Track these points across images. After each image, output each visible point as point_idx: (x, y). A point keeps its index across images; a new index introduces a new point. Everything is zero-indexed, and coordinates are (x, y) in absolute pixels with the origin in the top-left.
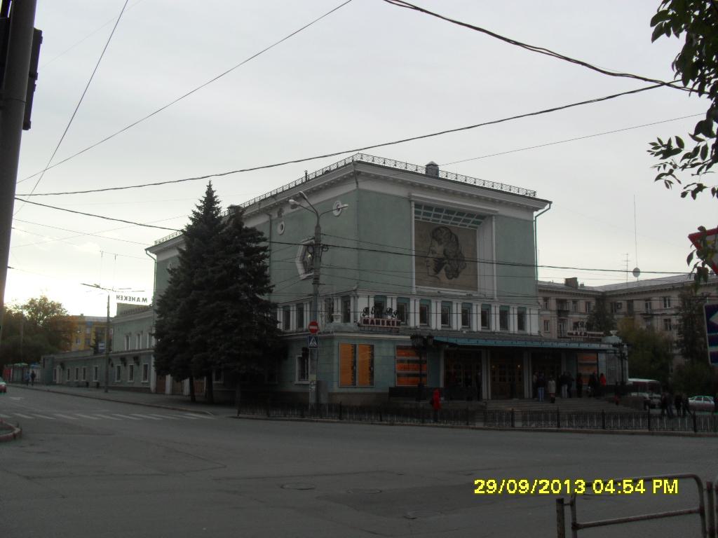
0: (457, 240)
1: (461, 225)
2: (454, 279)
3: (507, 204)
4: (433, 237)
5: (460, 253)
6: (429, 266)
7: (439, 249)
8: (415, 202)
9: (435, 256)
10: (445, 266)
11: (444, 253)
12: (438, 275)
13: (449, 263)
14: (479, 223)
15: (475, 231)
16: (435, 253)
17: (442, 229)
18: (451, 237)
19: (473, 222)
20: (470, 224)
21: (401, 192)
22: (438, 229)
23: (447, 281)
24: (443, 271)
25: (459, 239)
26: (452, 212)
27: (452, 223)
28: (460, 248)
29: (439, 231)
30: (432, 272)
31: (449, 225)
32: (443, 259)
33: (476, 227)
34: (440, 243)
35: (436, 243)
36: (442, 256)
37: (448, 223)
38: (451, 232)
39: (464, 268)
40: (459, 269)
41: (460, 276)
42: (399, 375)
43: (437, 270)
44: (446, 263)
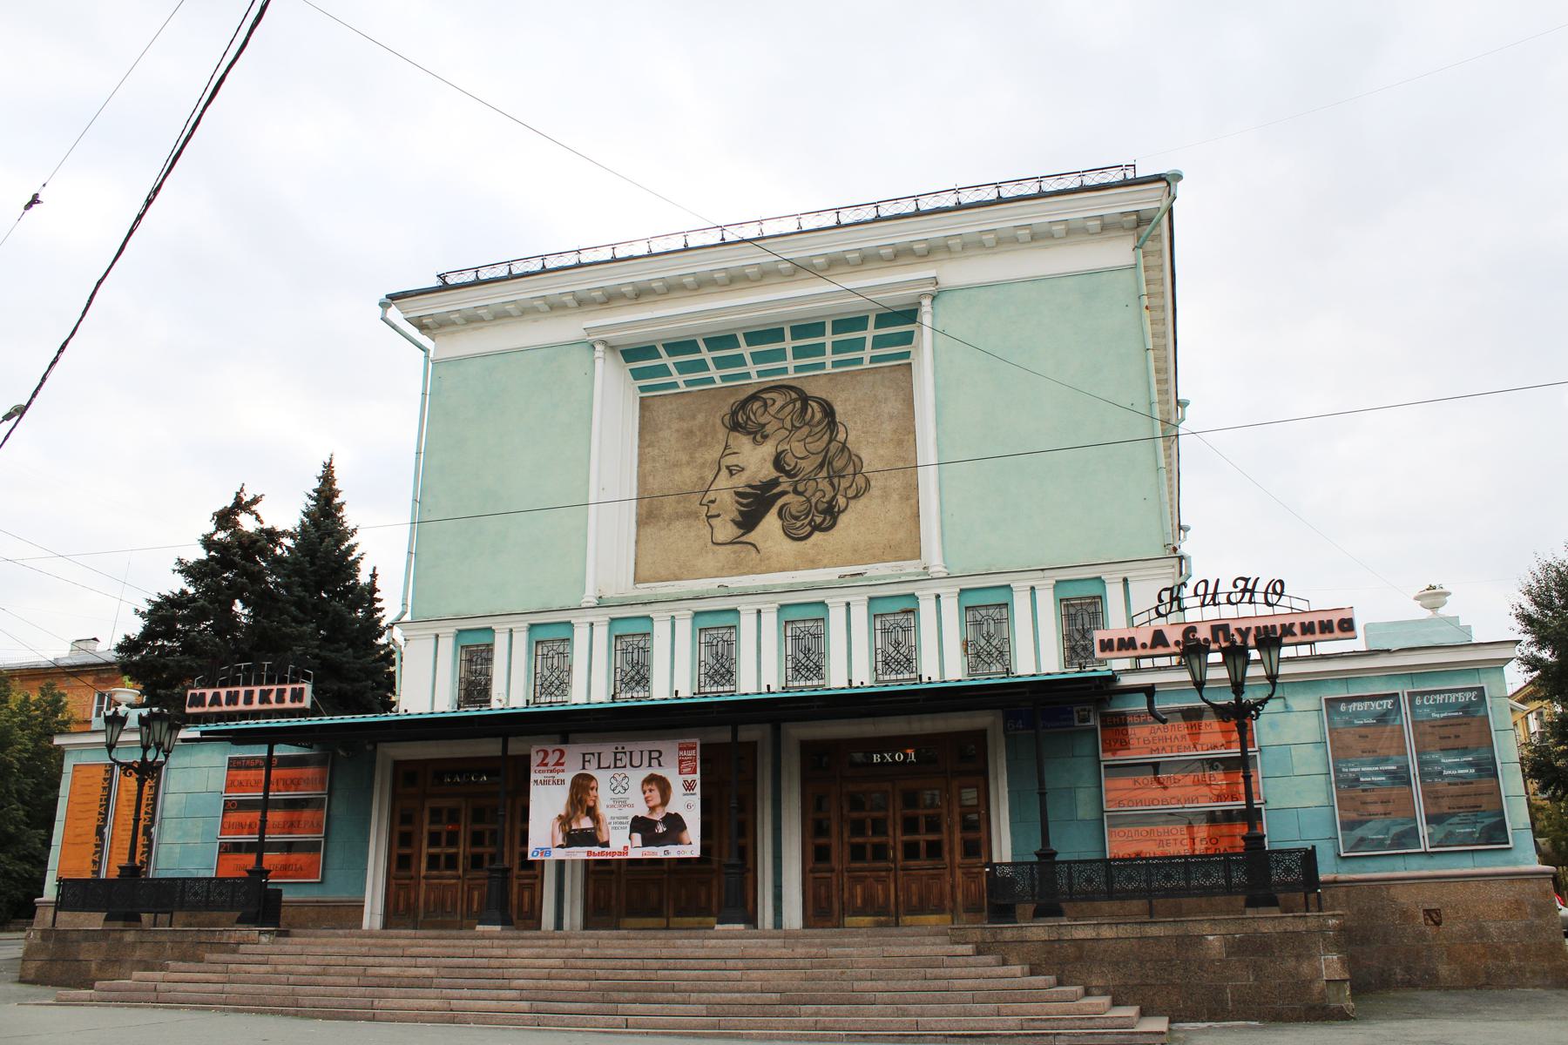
0: (829, 411)
1: (835, 364)
2: (817, 536)
3: (974, 246)
4: (735, 427)
5: (844, 447)
6: (709, 517)
7: (756, 461)
8: (604, 342)
9: (740, 481)
10: (780, 502)
11: (778, 462)
12: (751, 537)
13: (796, 492)
14: (908, 338)
15: (910, 364)
16: (743, 469)
17: (764, 396)
18: (804, 409)
19: (879, 342)
20: (868, 352)
21: (571, 328)
22: (754, 397)
23: (789, 546)
24: (771, 523)
25: (839, 409)
26: (775, 334)
27: (798, 369)
28: (841, 437)
29: (756, 405)
30: (725, 530)
31: (791, 374)
32: (774, 483)
33: (907, 355)
34: (759, 434)
35: (743, 443)
36: (768, 472)
37: (784, 370)
38: (805, 399)
39: (856, 497)
40: (841, 501)
41: (843, 520)
42: (226, 849)
43: (748, 520)
44: (784, 493)
